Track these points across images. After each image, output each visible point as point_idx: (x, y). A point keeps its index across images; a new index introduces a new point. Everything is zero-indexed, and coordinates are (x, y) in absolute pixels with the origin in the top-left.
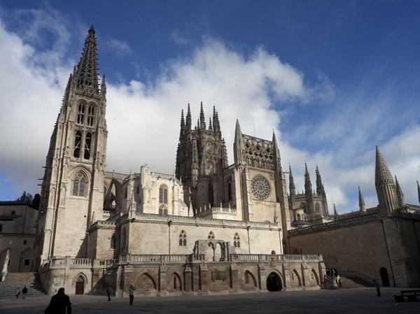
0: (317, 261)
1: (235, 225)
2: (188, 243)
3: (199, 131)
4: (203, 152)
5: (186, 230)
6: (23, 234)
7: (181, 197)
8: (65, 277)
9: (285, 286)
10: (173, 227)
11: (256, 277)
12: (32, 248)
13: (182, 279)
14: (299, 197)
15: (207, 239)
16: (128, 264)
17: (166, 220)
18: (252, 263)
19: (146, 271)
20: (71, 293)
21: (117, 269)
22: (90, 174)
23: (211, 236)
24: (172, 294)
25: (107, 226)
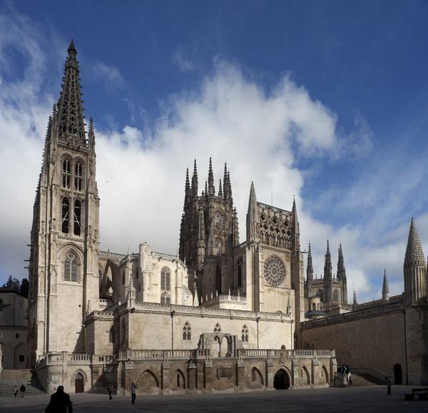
0: (329, 357)
1: (244, 315)
2: (192, 337)
3: (208, 197)
4: (211, 226)
5: (190, 322)
6: (14, 327)
7: (185, 282)
8: (63, 374)
9: (293, 384)
10: (176, 319)
11: (264, 374)
12: (25, 342)
13: (186, 377)
14: (317, 282)
15: (213, 332)
16: (129, 360)
17: (168, 310)
18: (260, 359)
19: (147, 367)
20: (71, 392)
21: (117, 365)
22: (82, 255)
23: (218, 327)
24: (175, 393)
25: (105, 316)
